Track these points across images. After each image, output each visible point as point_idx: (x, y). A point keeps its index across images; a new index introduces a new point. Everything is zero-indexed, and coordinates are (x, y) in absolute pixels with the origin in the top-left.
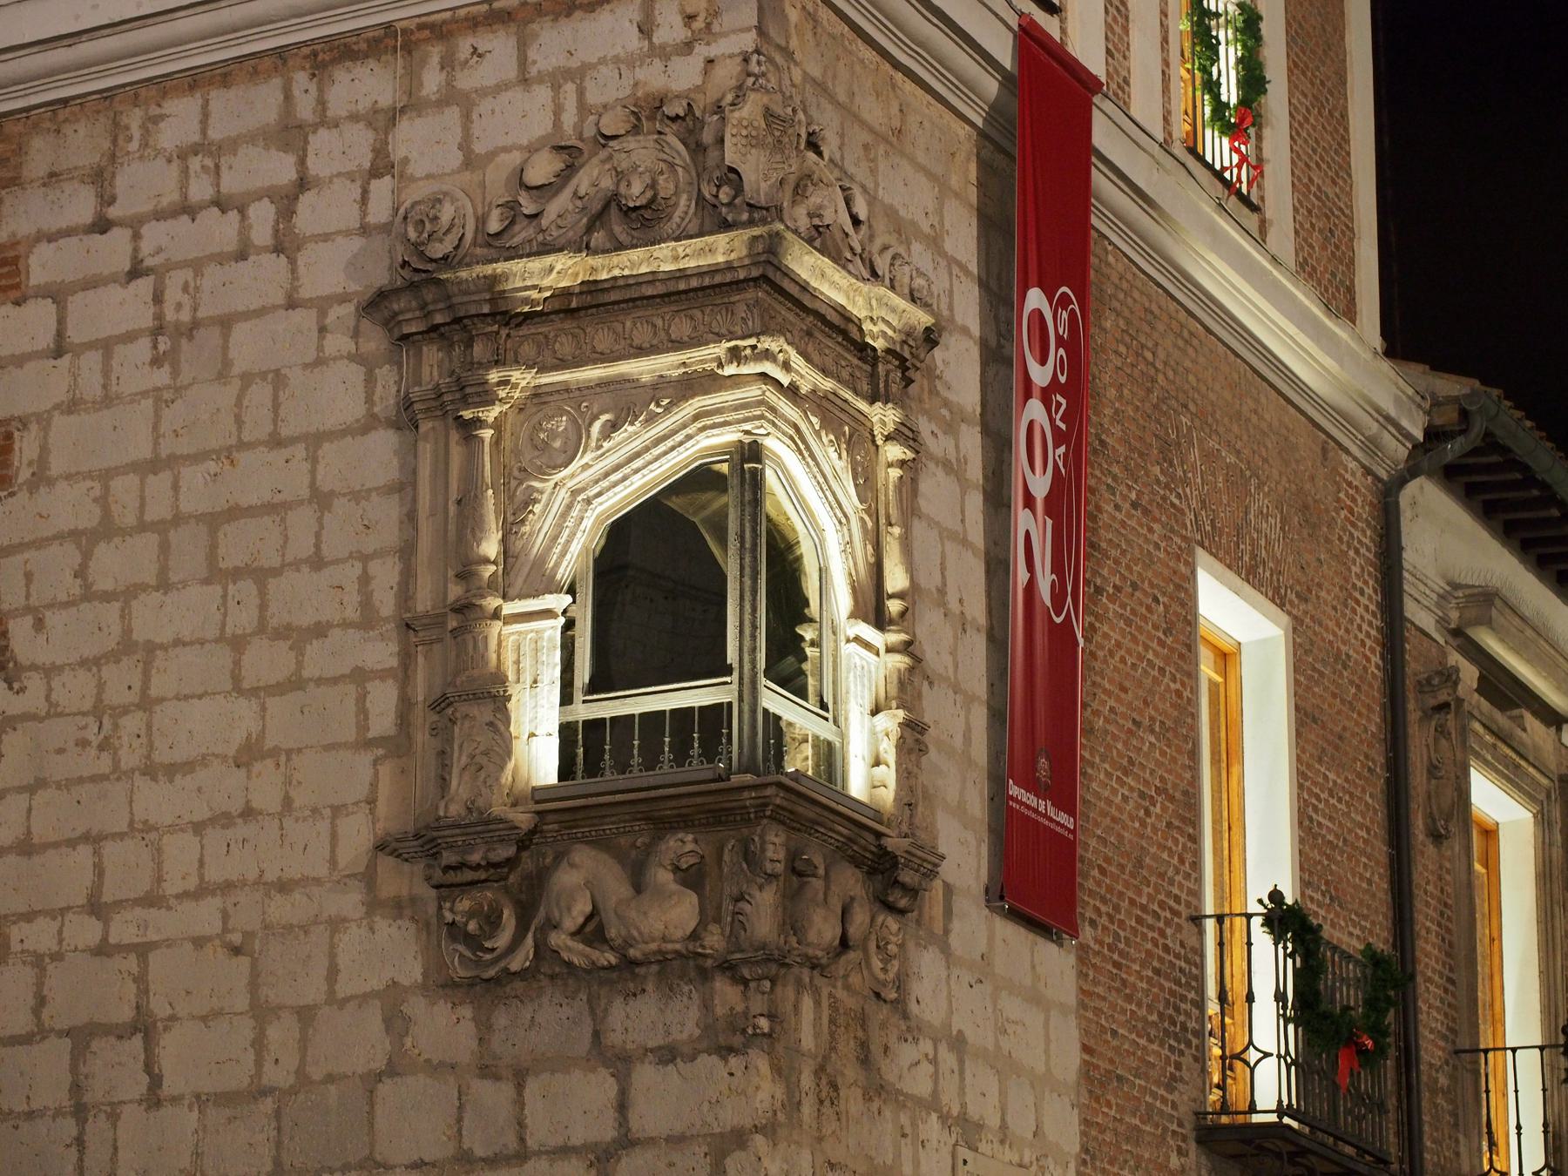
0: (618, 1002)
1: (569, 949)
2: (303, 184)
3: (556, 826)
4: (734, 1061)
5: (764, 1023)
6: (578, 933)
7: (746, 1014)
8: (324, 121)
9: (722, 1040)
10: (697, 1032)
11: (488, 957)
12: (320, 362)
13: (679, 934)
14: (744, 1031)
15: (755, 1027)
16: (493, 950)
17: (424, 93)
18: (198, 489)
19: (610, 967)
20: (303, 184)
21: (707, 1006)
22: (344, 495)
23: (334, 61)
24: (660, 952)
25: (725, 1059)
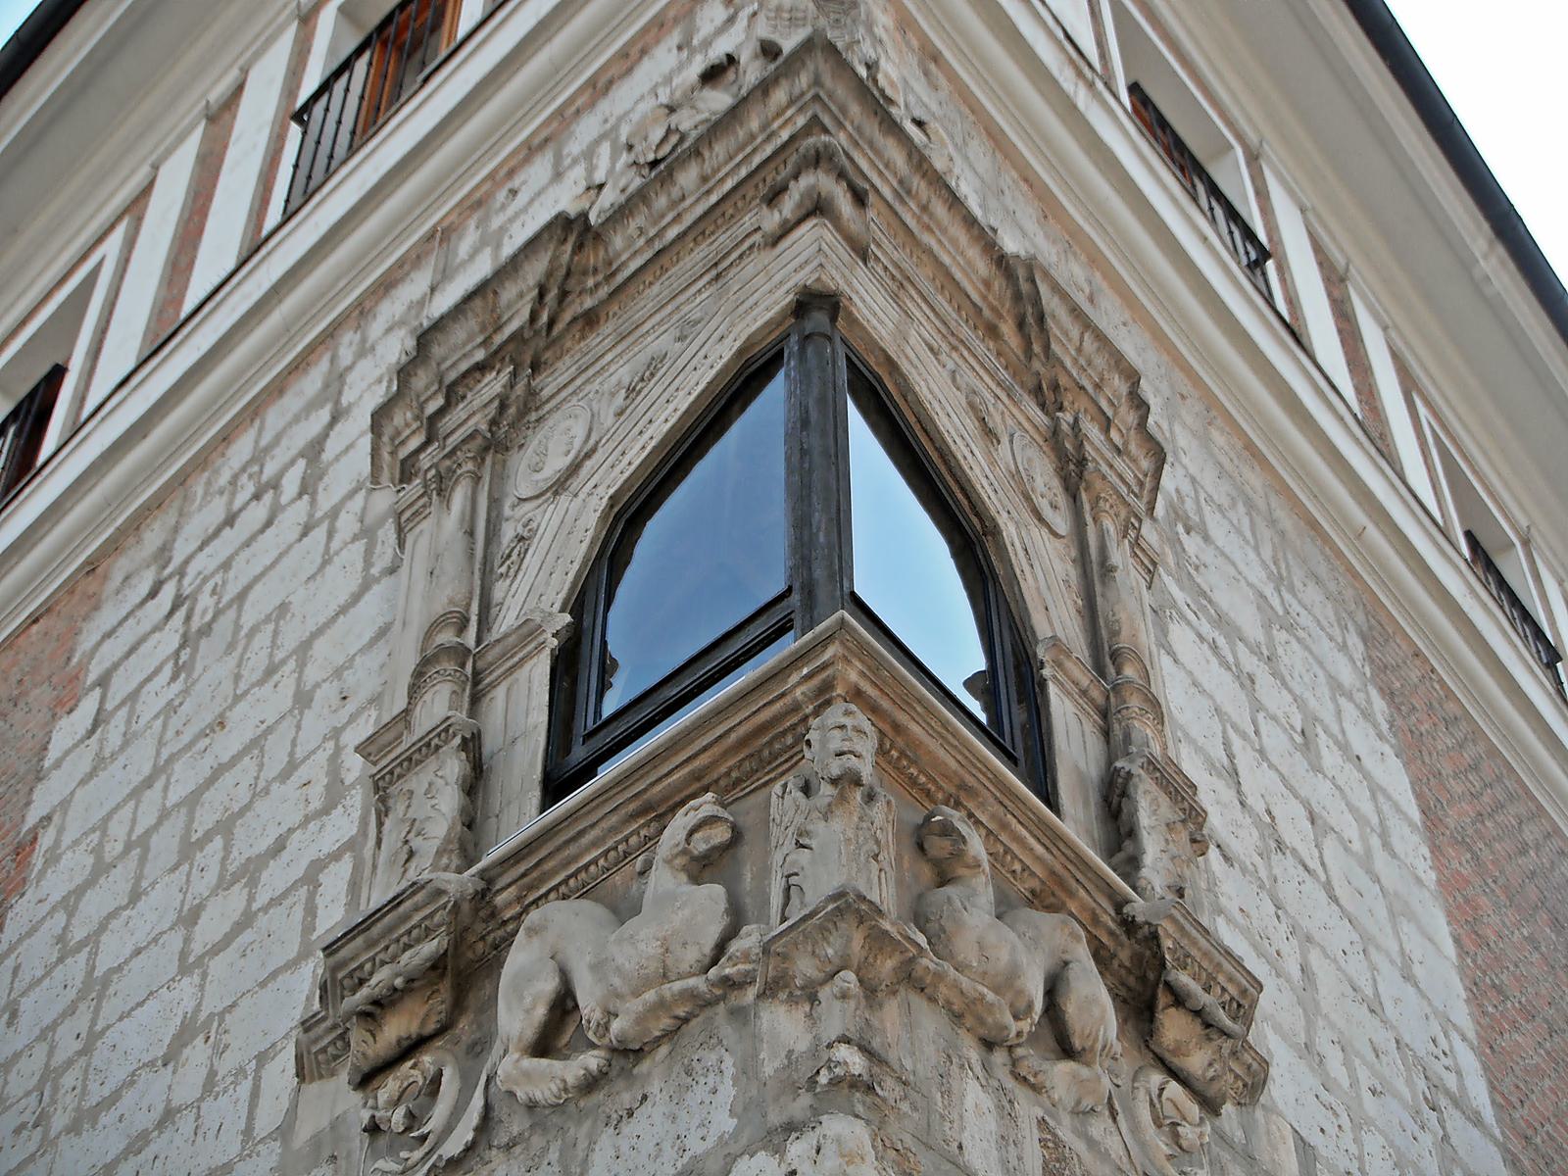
0: (606, 1138)
1: (527, 1075)
2: (334, 420)
3: (512, 891)
4: (798, 1150)
5: (854, 1061)
6: (543, 1046)
7: (814, 1051)
8: (364, 350)
9: (775, 1118)
10: (731, 1124)
11: (418, 1154)
12: (326, 561)
13: (691, 956)
14: (812, 1081)
15: (830, 1064)
16: (424, 1138)
17: (458, 260)
18: (185, 778)
19: (591, 1084)
20: (334, 420)
21: (747, 1069)
22: (324, 681)
23: (377, 303)
24: (661, 1005)
25: (779, 1151)
